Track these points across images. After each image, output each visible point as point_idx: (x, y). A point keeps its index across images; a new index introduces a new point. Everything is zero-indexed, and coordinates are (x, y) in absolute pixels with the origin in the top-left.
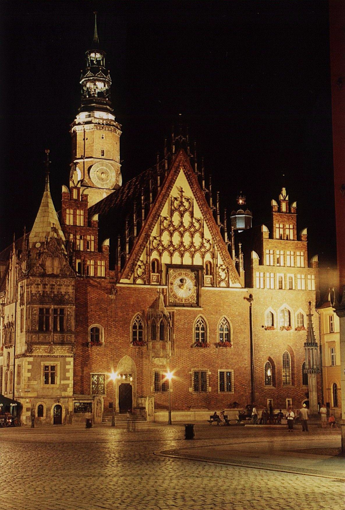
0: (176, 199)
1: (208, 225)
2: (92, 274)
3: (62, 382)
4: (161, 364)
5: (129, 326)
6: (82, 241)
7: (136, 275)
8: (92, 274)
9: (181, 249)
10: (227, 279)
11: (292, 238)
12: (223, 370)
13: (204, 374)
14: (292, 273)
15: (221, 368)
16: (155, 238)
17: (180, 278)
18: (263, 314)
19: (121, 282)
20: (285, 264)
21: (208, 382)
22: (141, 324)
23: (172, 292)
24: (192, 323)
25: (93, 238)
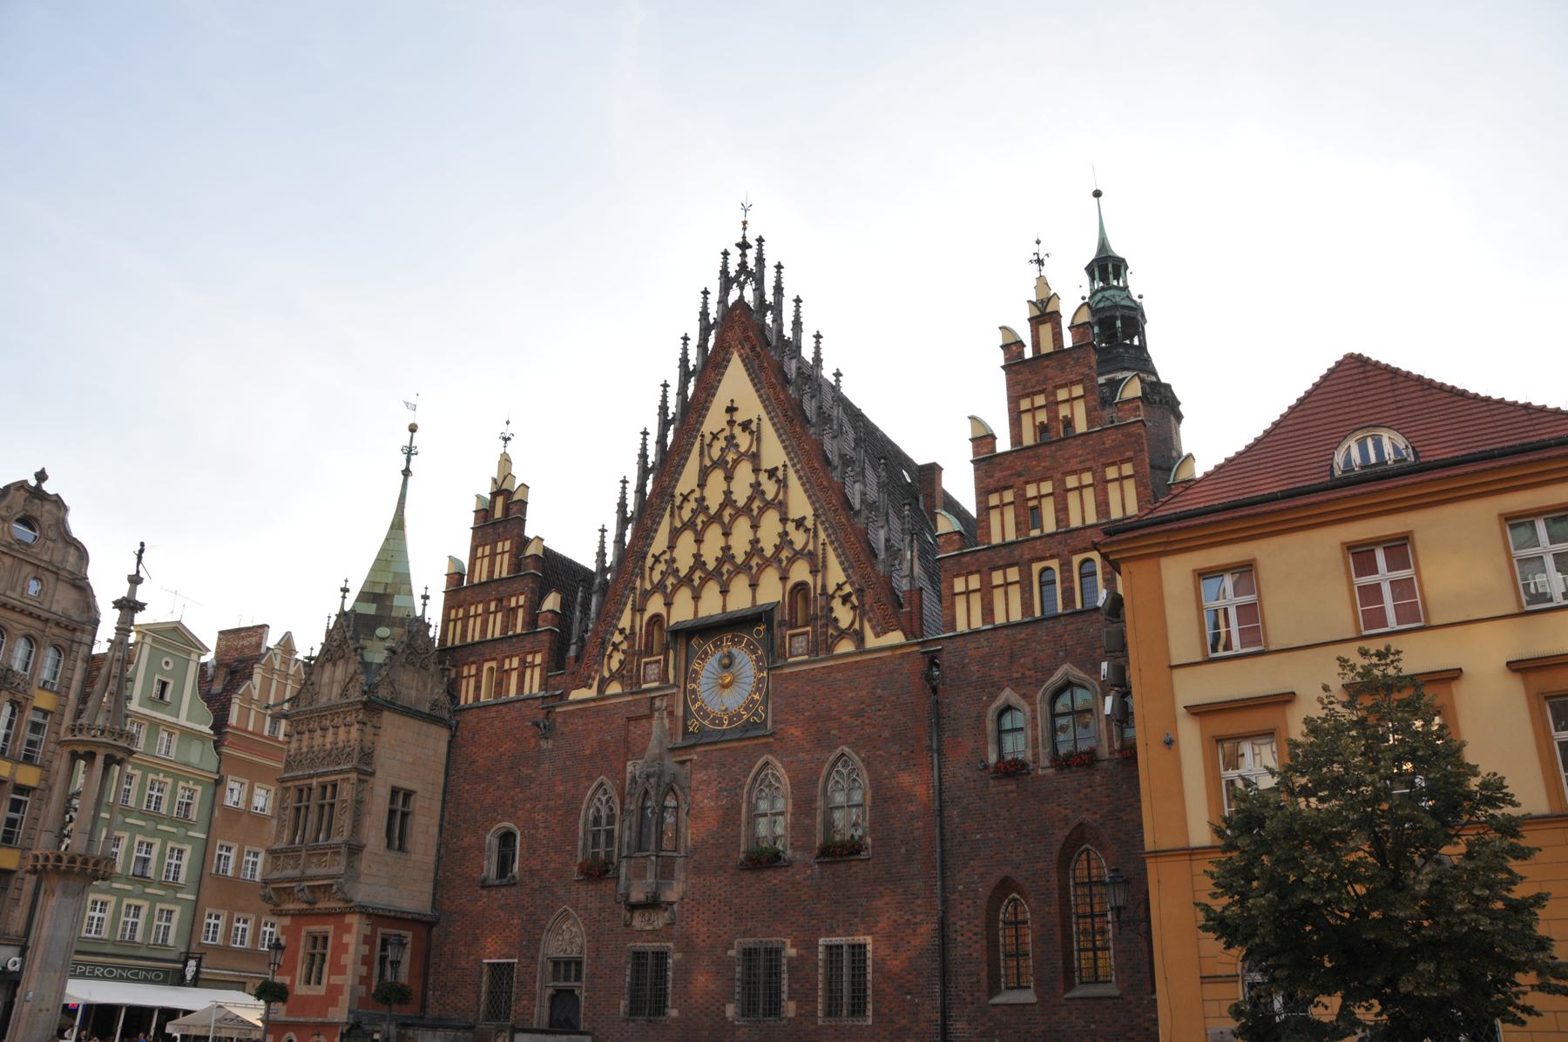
0: (715, 437)
1: (800, 478)
2: (512, 693)
3: (335, 980)
4: (649, 928)
5: (576, 820)
6: (499, 616)
7: (607, 674)
8: (512, 693)
9: (723, 572)
10: (857, 626)
11: (1081, 426)
12: (835, 940)
13: (774, 954)
14: (1085, 550)
15: (830, 932)
16: (657, 559)
17: (718, 656)
18: (981, 718)
19: (571, 697)
20: (1058, 521)
21: (785, 982)
22: (611, 809)
23: (695, 701)
24: (742, 787)
25: (522, 600)
